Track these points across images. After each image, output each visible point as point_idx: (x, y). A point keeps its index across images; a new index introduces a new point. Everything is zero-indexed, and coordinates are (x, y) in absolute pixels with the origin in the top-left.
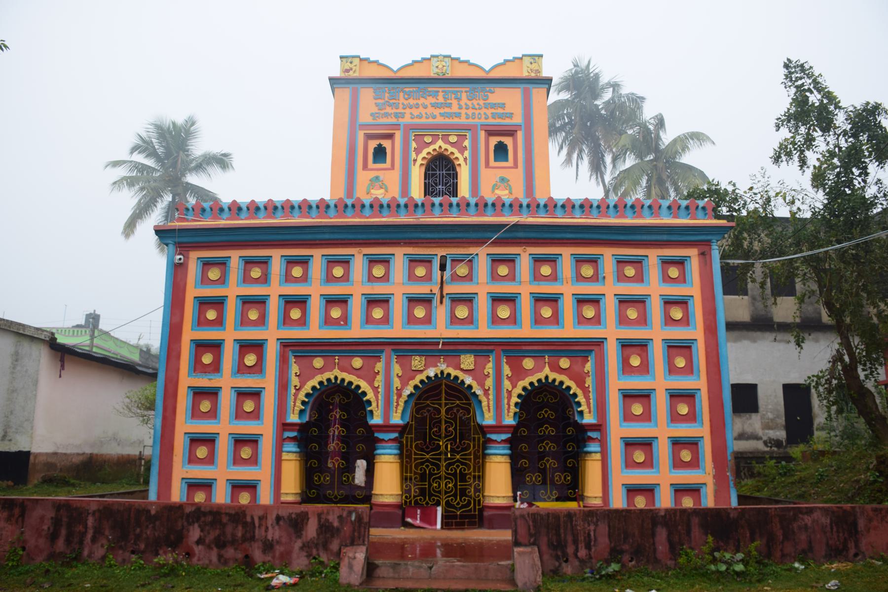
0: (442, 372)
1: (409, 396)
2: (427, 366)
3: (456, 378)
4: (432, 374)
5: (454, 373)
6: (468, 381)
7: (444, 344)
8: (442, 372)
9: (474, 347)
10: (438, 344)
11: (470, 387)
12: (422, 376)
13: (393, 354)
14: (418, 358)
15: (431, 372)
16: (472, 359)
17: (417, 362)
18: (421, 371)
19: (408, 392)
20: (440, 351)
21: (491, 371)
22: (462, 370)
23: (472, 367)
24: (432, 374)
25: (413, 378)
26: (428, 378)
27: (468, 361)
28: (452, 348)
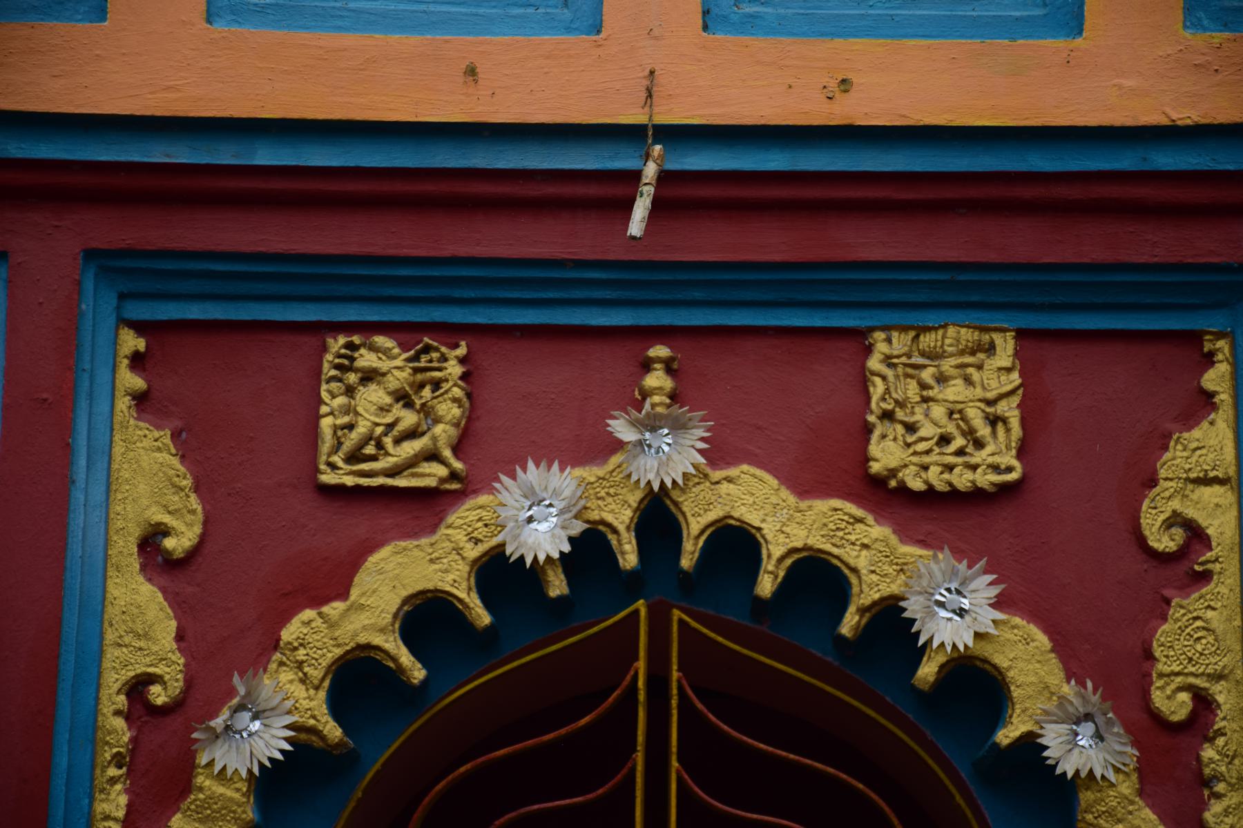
0: (658, 518)
1: (274, 783)
2: (484, 454)
3: (818, 578)
4: (543, 538)
5: (786, 521)
6: (958, 613)
7: (678, 194)
8: (658, 518)
9: (1020, 242)
10: (615, 192)
11: (976, 685)
12: (437, 562)
13: (97, 304)
14: (387, 358)
15: (538, 515)
16: (1000, 371)
17: (376, 403)
18: (423, 508)
19: (267, 741)
20: (640, 277)
21: (1216, 512)
22: (883, 495)
23: (997, 461)
24: (543, 538)
25: (331, 581)
26: (500, 573)
27: (950, 399)
28: (771, 242)
